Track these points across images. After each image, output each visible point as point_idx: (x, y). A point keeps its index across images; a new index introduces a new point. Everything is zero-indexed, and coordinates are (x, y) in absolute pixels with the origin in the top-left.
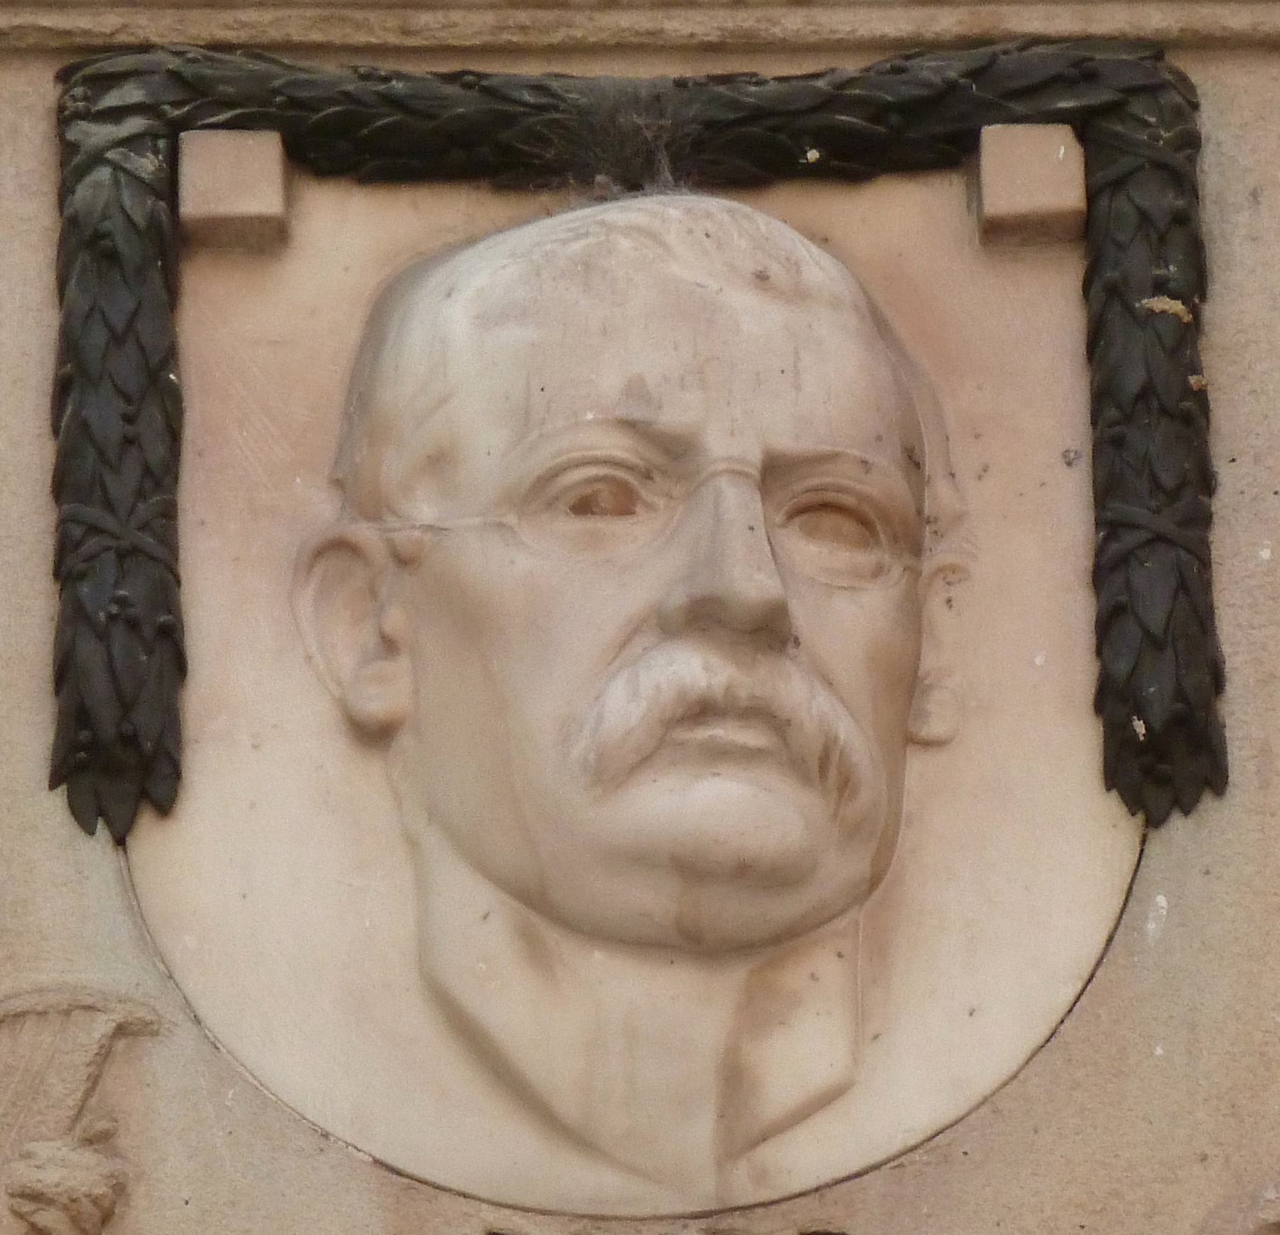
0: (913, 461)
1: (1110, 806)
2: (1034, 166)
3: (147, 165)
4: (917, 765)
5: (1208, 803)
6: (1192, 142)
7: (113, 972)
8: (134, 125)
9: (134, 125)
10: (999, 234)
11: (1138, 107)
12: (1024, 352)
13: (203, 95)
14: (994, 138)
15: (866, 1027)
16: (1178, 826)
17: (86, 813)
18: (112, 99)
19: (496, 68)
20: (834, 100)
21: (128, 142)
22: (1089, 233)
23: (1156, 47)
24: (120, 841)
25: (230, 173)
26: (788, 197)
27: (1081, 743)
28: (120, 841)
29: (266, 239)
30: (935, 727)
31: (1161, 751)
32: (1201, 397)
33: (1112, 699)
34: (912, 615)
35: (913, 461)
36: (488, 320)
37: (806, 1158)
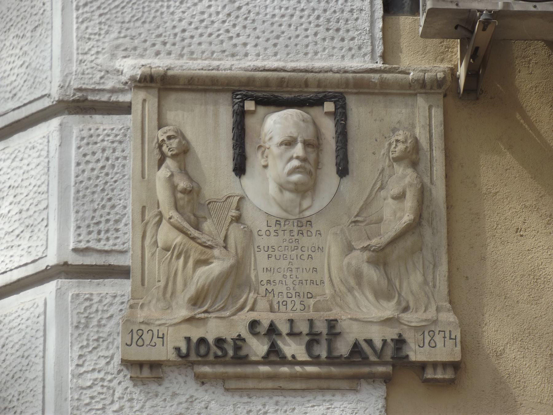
0: (318, 138)
1: (337, 176)
2: (329, 106)
3: (241, 104)
4: (318, 171)
5: (347, 176)
6: (345, 104)
7: (239, 192)
8: (240, 100)
9: (240, 100)
10: (327, 114)
11: (340, 100)
12: (329, 127)
13: (246, 97)
14: (326, 104)
15: (313, 200)
16: (344, 178)
17: (236, 175)
18: (238, 97)
19: (276, 94)
20: (309, 99)
21: (240, 102)
22: (334, 114)
23: (341, 93)
24: (240, 178)
25: (250, 105)
26: (306, 109)
27: (334, 169)
28: (240, 178)
29: (253, 113)
30: (320, 167)
31: (343, 170)
32: (346, 132)
33: (338, 165)
34: (318, 156)
35: (318, 138)
36: (275, 122)
37: (307, 213)
